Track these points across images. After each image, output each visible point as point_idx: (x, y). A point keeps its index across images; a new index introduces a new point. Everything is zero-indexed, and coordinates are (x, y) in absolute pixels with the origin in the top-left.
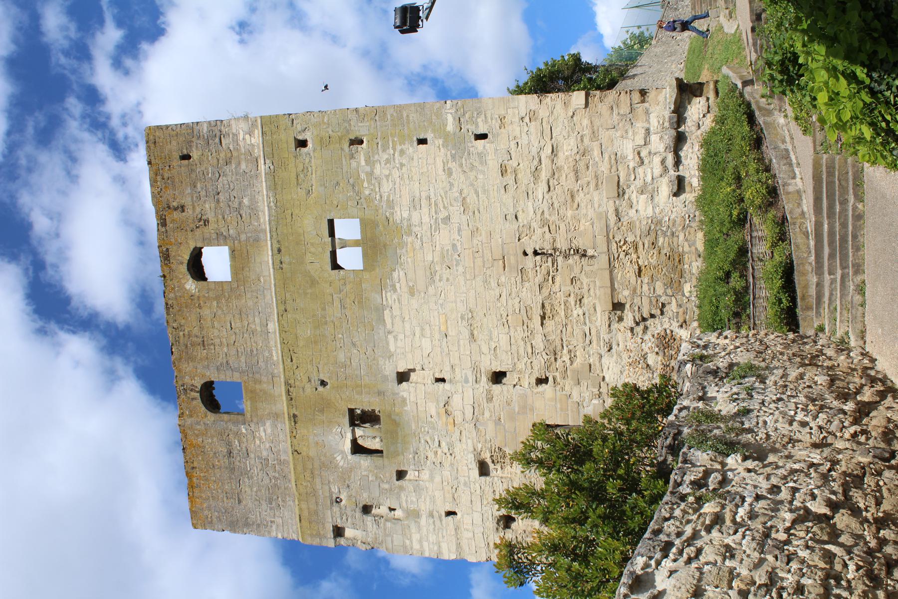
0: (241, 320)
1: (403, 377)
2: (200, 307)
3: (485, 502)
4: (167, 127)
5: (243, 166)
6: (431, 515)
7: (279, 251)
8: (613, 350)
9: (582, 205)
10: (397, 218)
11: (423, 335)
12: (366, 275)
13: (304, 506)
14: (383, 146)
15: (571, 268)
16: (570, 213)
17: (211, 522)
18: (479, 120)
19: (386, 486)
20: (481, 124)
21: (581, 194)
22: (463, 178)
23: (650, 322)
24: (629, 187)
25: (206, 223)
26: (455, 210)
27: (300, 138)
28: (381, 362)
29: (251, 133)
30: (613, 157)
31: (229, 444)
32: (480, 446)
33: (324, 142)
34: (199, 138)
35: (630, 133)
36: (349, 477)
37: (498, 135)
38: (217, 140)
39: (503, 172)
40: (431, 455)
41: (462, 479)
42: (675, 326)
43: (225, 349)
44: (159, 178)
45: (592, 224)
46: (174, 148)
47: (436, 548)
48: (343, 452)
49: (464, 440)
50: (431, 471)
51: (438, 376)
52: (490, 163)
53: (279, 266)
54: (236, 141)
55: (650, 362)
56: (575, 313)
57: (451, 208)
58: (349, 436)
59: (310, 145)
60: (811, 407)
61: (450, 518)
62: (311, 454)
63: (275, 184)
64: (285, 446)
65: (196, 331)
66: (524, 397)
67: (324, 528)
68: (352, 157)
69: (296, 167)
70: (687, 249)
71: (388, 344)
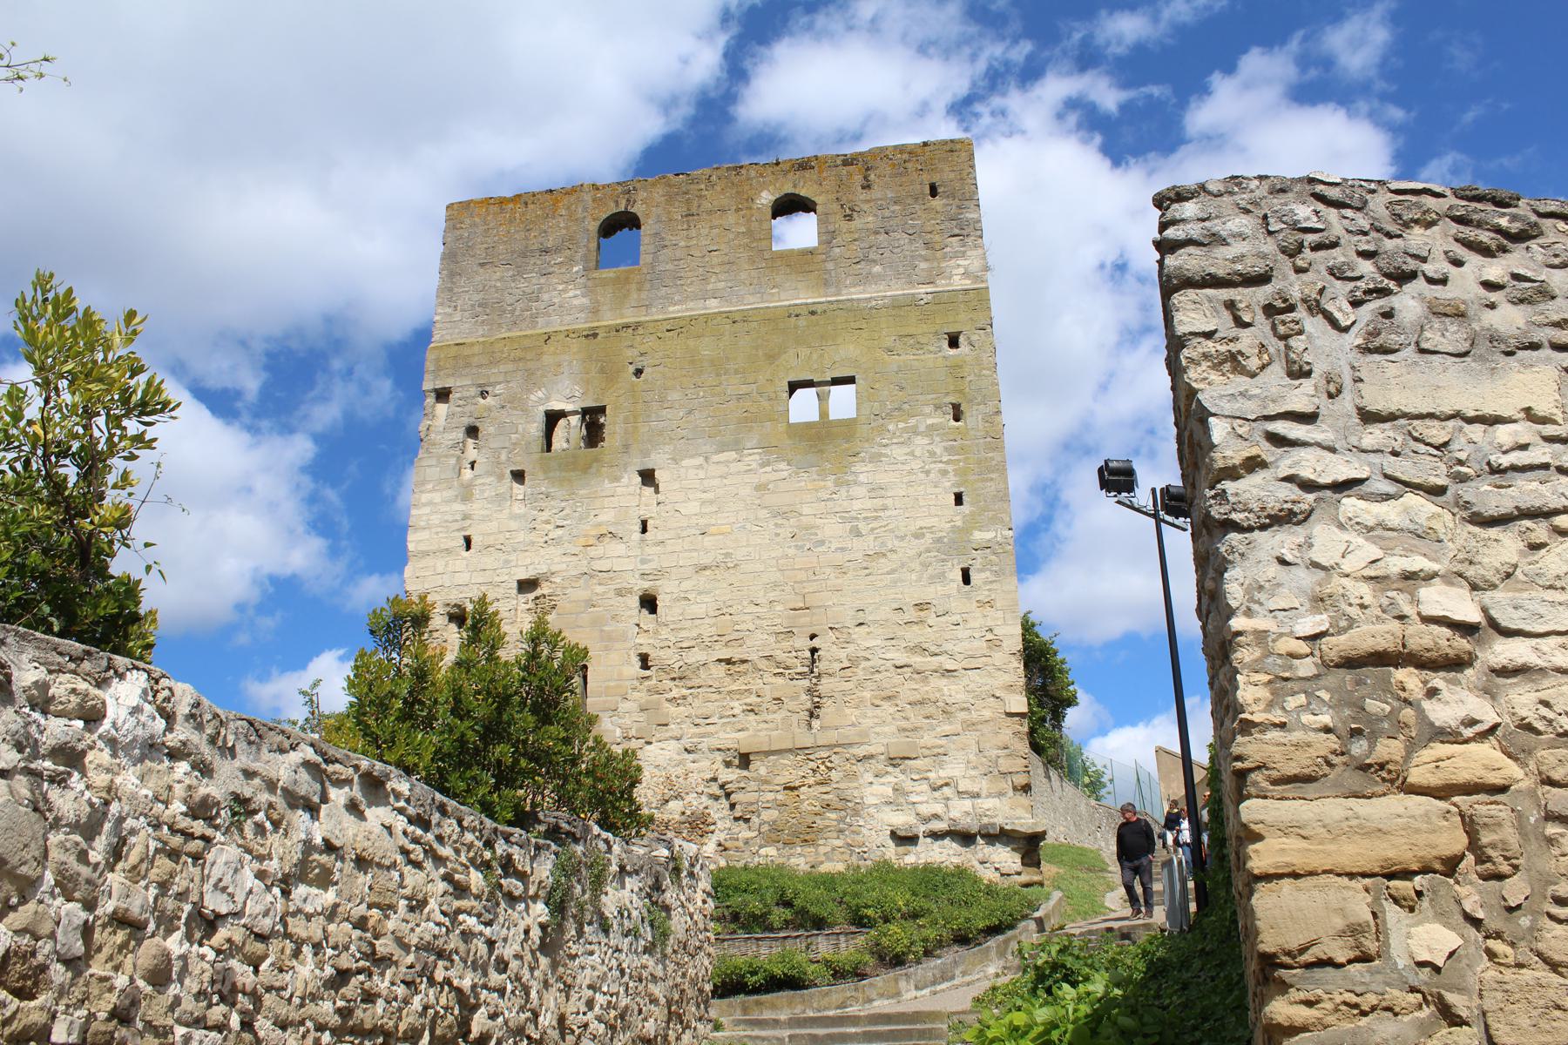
0: (723, 264)
1: (648, 477)
2: (738, 210)
4: (973, 167)
5: (923, 265)
6: (466, 517)
7: (813, 313)
8: (686, 755)
9: (878, 711)
10: (858, 468)
11: (703, 503)
12: (782, 427)
13: (476, 349)
14: (952, 447)
15: (795, 697)
16: (867, 694)
17: (455, 228)
19: (503, 457)
20: (983, 575)
21: (893, 710)
22: (911, 553)
23: (724, 803)
24: (903, 772)
25: (849, 218)
26: (869, 544)
27: (961, 339)
28: (668, 448)
29: (966, 274)
30: (941, 751)
31: (557, 250)
32: (558, 580)
33: (955, 370)
34: (959, 207)
35: (973, 773)
38: (957, 231)
39: (920, 606)
40: (545, 515)
41: (513, 557)
42: (722, 837)
43: (682, 244)
44: (906, 156)
45: (853, 725)
46: (945, 176)
48: (548, 399)
49: (565, 559)
52: (932, 589)
53: (793, 313)
54: (956, 256)
55: (671, 804)
56: (736, 704)
57: (872, 537)
58: (569, 407)
59: (953, 352)
60: (613, 1013)
61: (463, 542)
63: (900, 307)
64: (556, 323)
65: (706, 205)
66: (624, 637)
67: (448, 376)
68: (937, 407)
69: (923, 334)
70: (822, 850)
71: (692, 457)
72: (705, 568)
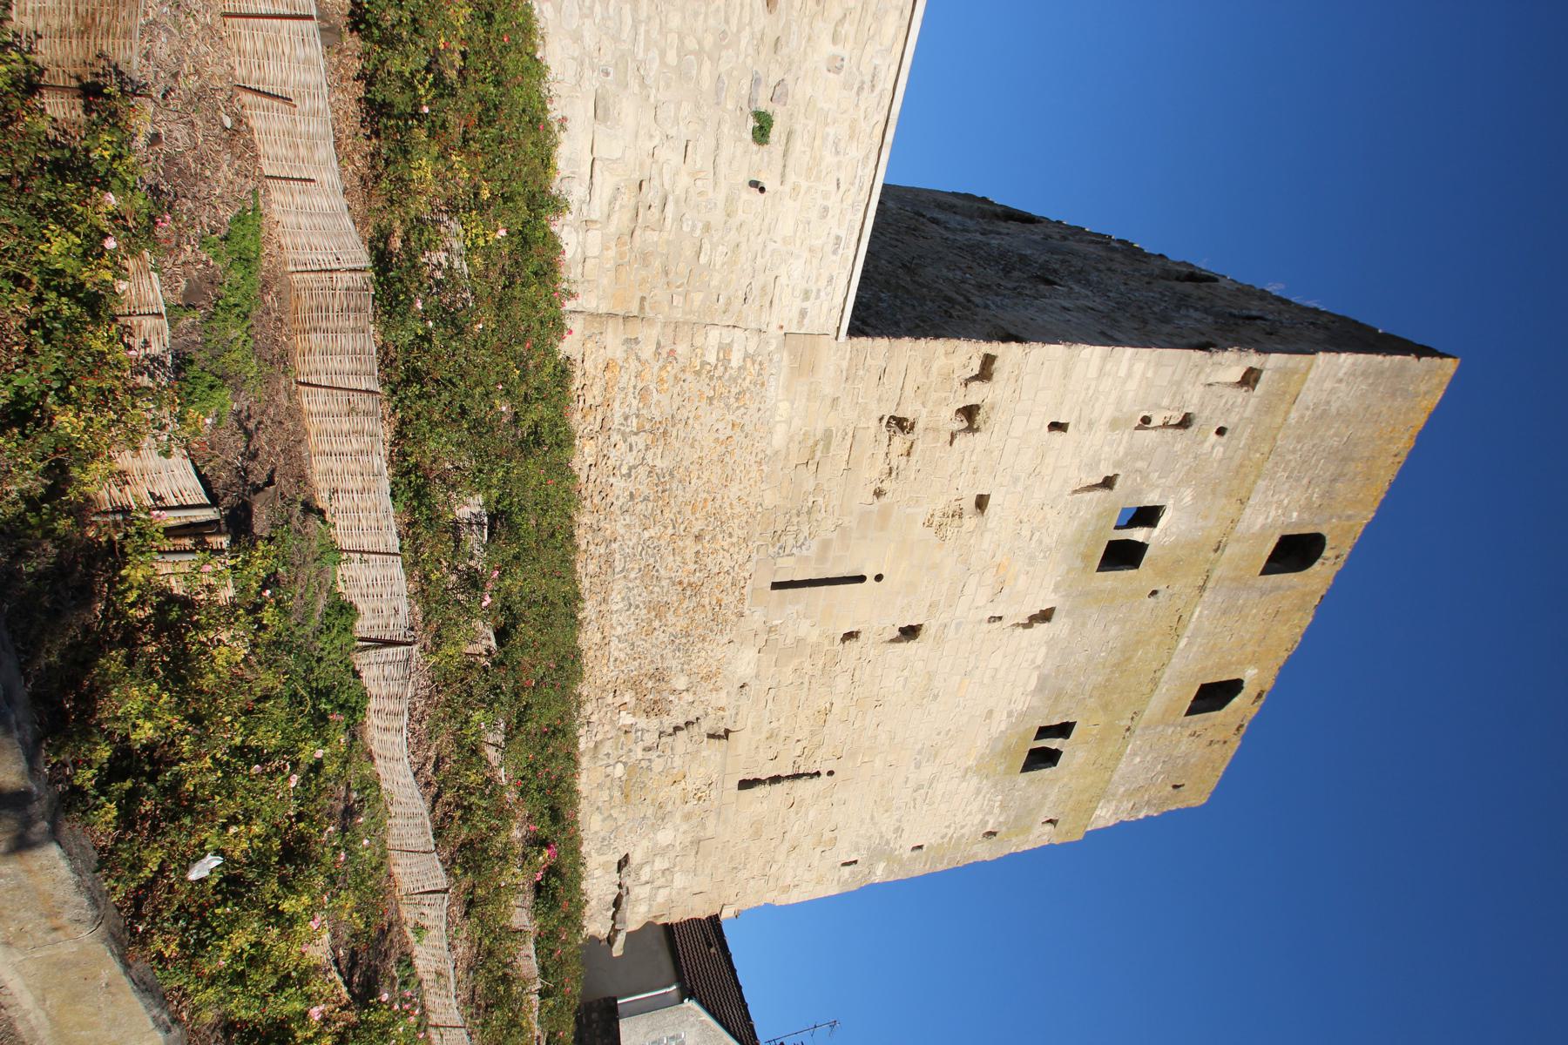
1: (1046, 616)
36: (1187, 473)
41: (1020, 488)
47: (1108, 367)
48: (1175, 509)
70: (615, 813)
72: (930, 680)
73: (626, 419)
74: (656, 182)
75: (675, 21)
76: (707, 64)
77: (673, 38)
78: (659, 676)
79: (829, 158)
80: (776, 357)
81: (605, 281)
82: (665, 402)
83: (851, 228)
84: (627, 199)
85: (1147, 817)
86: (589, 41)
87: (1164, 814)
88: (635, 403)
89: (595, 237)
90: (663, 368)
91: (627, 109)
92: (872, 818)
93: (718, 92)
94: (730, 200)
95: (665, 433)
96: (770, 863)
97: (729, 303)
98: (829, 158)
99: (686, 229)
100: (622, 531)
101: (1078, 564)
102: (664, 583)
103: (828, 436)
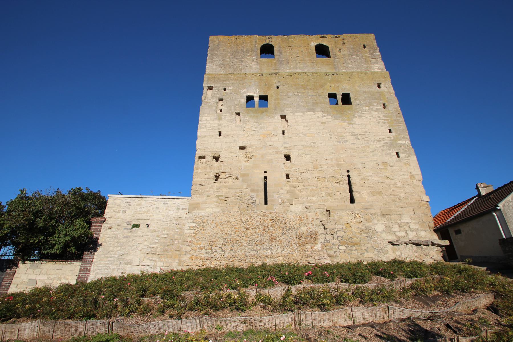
3: (226, 149)
5: (365, 65)
6: (219, 125)
10: (355, 119)
18: (405, 154)
19: (233, 108)
24: (388, 220)
25: (340, 51)
27: (382, 86)
28: (290, 109)
30: (401, 213)
31: (247, 52)
37: (401, 162)
47: (203, 126)
50: (241, 126)
51: (286, 132)
54: (374, 64)
61: (218, 133)
62: (246, 80)
64: (248, 71)
70: (364, 248)
73: (207, 253)
74: (146, 250)
75: (111, 248)
76: (120, 240)
77: (115, 248)
78: (299, 237)
79: (145, 209)
80: (194, 214)
81: (170, 261)
82: (204, 242)
83: (161, 201)
84: (149, 256)
85: (380, 52)
86: (114, 267)
87: (378, 45)
88: (203, 251)
89: (158, 264)
90: (194, 244)
91: (129, 258)
92: (372, 152)
93: (127, 237)
94: (151, 231)
95: (212, 242)
96: (397, 186)
97: (179, 228)
98: (145, 209)
99: (157, 241)
100: (243, 252)
101: (264, 114)
102: (262, 238)
103: (218, 196)
